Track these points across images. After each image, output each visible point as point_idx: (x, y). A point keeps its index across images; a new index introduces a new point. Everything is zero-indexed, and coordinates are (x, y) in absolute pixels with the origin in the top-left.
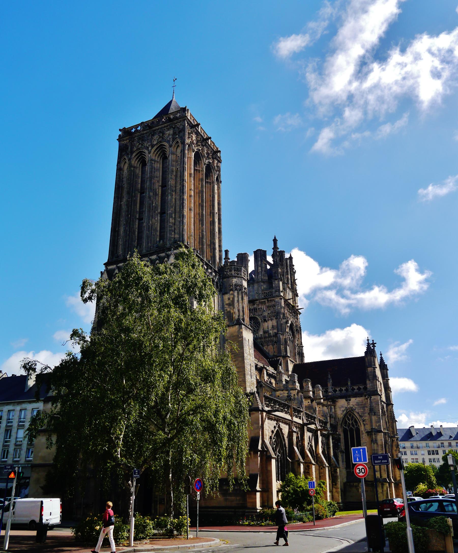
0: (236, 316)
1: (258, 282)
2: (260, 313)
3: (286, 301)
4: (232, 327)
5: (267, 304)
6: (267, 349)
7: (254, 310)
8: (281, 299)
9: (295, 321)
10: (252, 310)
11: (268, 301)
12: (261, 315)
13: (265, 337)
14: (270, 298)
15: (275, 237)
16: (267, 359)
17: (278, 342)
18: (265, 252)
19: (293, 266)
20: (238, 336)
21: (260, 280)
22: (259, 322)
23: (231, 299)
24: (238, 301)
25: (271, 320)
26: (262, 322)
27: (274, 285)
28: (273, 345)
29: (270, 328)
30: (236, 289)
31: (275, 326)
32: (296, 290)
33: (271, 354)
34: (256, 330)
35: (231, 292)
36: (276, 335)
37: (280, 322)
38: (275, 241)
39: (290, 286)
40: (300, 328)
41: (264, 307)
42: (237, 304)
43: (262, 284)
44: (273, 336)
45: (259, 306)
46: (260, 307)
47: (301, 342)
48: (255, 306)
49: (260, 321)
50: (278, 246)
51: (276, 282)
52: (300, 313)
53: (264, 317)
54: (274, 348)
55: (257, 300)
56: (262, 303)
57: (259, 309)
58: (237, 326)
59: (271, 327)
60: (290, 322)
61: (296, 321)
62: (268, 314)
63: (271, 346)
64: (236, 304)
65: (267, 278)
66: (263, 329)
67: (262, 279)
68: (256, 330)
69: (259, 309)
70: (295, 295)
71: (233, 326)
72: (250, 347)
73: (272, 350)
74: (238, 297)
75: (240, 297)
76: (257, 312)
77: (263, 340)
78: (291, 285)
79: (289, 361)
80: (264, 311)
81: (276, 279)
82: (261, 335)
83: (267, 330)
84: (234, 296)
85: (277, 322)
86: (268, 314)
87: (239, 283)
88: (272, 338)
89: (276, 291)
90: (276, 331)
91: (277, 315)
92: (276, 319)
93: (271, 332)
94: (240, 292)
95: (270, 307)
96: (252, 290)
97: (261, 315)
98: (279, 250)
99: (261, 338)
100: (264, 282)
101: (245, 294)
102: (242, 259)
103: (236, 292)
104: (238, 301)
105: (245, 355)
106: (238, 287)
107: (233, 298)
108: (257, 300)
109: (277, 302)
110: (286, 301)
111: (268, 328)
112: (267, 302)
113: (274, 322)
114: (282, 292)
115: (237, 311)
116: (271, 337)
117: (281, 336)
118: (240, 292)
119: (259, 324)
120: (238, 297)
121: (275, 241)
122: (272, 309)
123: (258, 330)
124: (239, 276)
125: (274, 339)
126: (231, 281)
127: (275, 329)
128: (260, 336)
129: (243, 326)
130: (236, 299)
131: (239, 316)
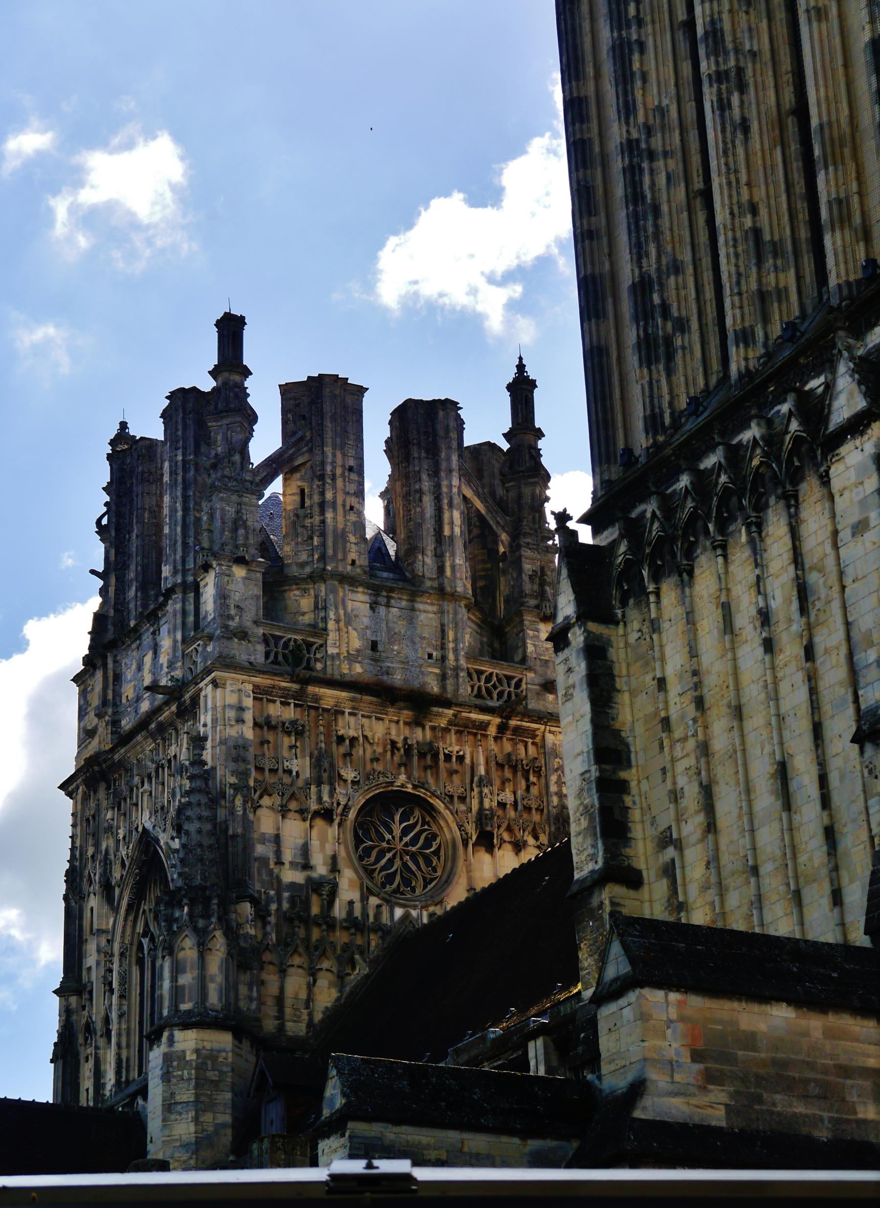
11: (502, 728)
15: (521, 367)
55: (448, 704)
112: (492, 731)
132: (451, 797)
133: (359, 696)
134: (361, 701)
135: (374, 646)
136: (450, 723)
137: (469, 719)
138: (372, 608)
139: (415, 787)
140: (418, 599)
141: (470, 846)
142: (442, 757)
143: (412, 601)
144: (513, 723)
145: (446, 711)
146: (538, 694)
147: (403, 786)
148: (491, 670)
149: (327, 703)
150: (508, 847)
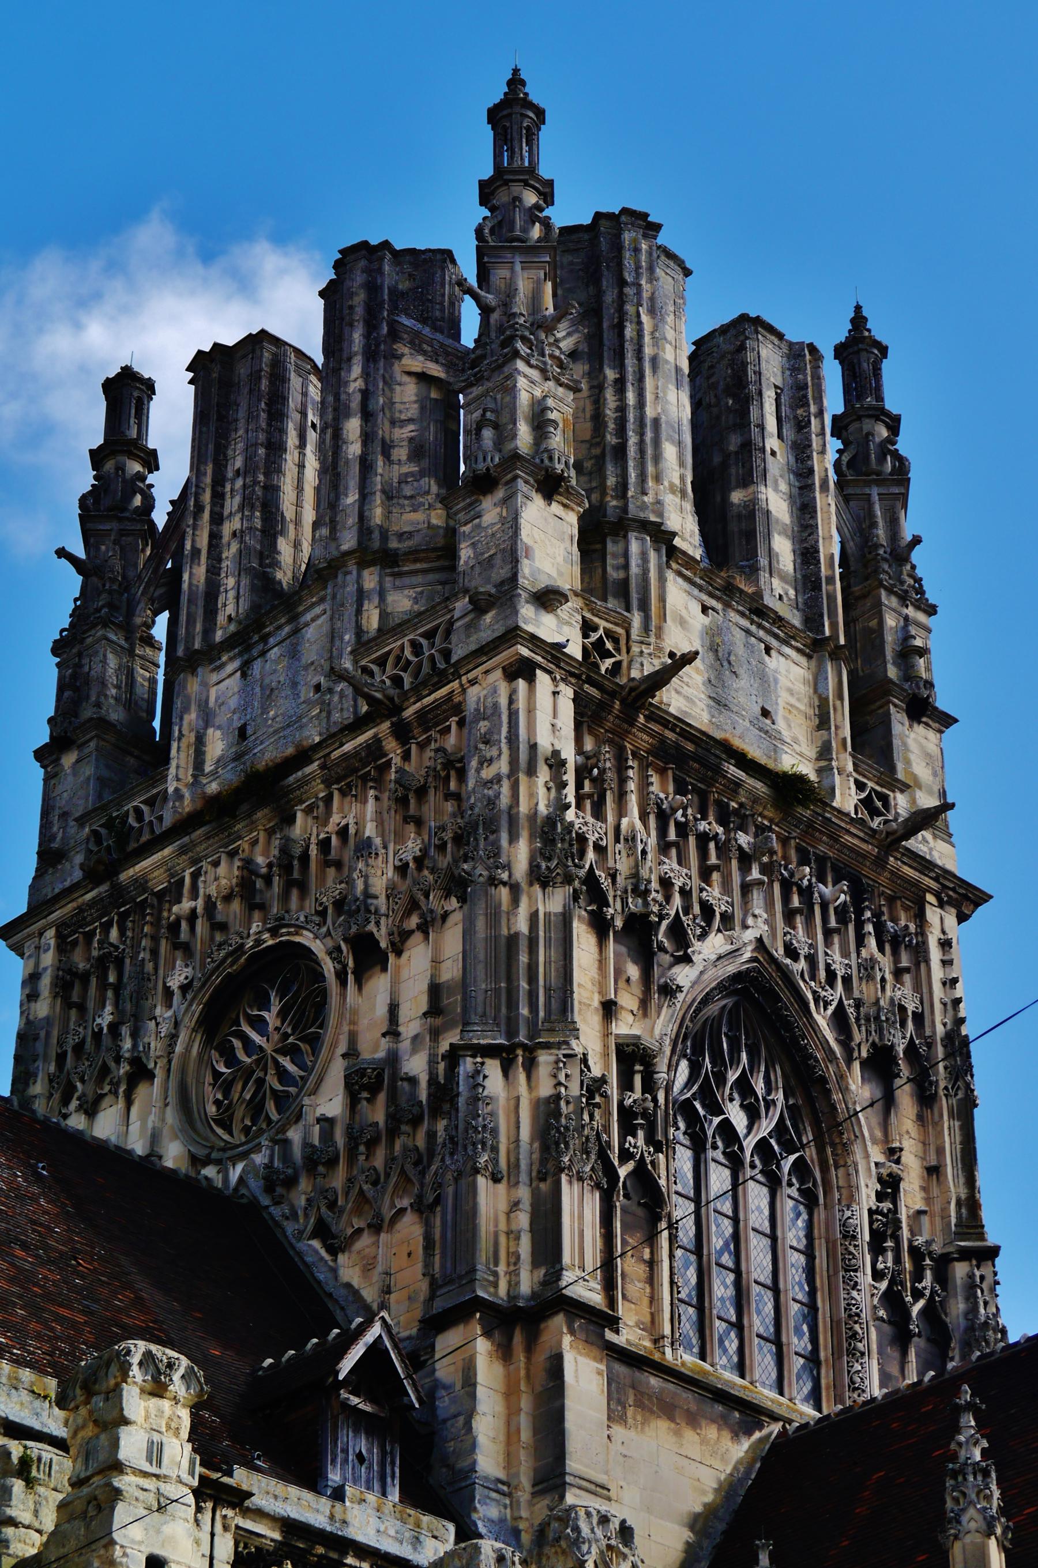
6: (368, 1268)
11: (402, 733)
14: (418, 691)
26: (341, 977)
29: (411, 1025)
37: (494, 916)
38: (514, 118)
40: (958, 1046)
47: (971, 1205)
50: (553, 154)
59: (423, 1004)
62: (402, 869)
66: (351, 1053)
69: (325, 845)
70: (882, 694)
76: (303, 887)
89: (480, 606)
93: (416, 1065)
99: (318, 1160)
108: (303, 756)
109: (480, 715)
110: (616, 704)
111: (393, 1032)
112: (392, 747)
114: (548, 599)
121: (514, 118)
133: (186, 839)
134: (193, 844)
137: (346, 757)
138: (244, 675)
139: (274, 932)
140: (301, 608)
141: (351, 978)
142: (313, 850)
143: (294, 618)
144: (409, 712)
145: (308, 770)
146: (468, 626)
147: (258, 942)
148: (399, 643)
149: (159, 882)
150: (418, 937)
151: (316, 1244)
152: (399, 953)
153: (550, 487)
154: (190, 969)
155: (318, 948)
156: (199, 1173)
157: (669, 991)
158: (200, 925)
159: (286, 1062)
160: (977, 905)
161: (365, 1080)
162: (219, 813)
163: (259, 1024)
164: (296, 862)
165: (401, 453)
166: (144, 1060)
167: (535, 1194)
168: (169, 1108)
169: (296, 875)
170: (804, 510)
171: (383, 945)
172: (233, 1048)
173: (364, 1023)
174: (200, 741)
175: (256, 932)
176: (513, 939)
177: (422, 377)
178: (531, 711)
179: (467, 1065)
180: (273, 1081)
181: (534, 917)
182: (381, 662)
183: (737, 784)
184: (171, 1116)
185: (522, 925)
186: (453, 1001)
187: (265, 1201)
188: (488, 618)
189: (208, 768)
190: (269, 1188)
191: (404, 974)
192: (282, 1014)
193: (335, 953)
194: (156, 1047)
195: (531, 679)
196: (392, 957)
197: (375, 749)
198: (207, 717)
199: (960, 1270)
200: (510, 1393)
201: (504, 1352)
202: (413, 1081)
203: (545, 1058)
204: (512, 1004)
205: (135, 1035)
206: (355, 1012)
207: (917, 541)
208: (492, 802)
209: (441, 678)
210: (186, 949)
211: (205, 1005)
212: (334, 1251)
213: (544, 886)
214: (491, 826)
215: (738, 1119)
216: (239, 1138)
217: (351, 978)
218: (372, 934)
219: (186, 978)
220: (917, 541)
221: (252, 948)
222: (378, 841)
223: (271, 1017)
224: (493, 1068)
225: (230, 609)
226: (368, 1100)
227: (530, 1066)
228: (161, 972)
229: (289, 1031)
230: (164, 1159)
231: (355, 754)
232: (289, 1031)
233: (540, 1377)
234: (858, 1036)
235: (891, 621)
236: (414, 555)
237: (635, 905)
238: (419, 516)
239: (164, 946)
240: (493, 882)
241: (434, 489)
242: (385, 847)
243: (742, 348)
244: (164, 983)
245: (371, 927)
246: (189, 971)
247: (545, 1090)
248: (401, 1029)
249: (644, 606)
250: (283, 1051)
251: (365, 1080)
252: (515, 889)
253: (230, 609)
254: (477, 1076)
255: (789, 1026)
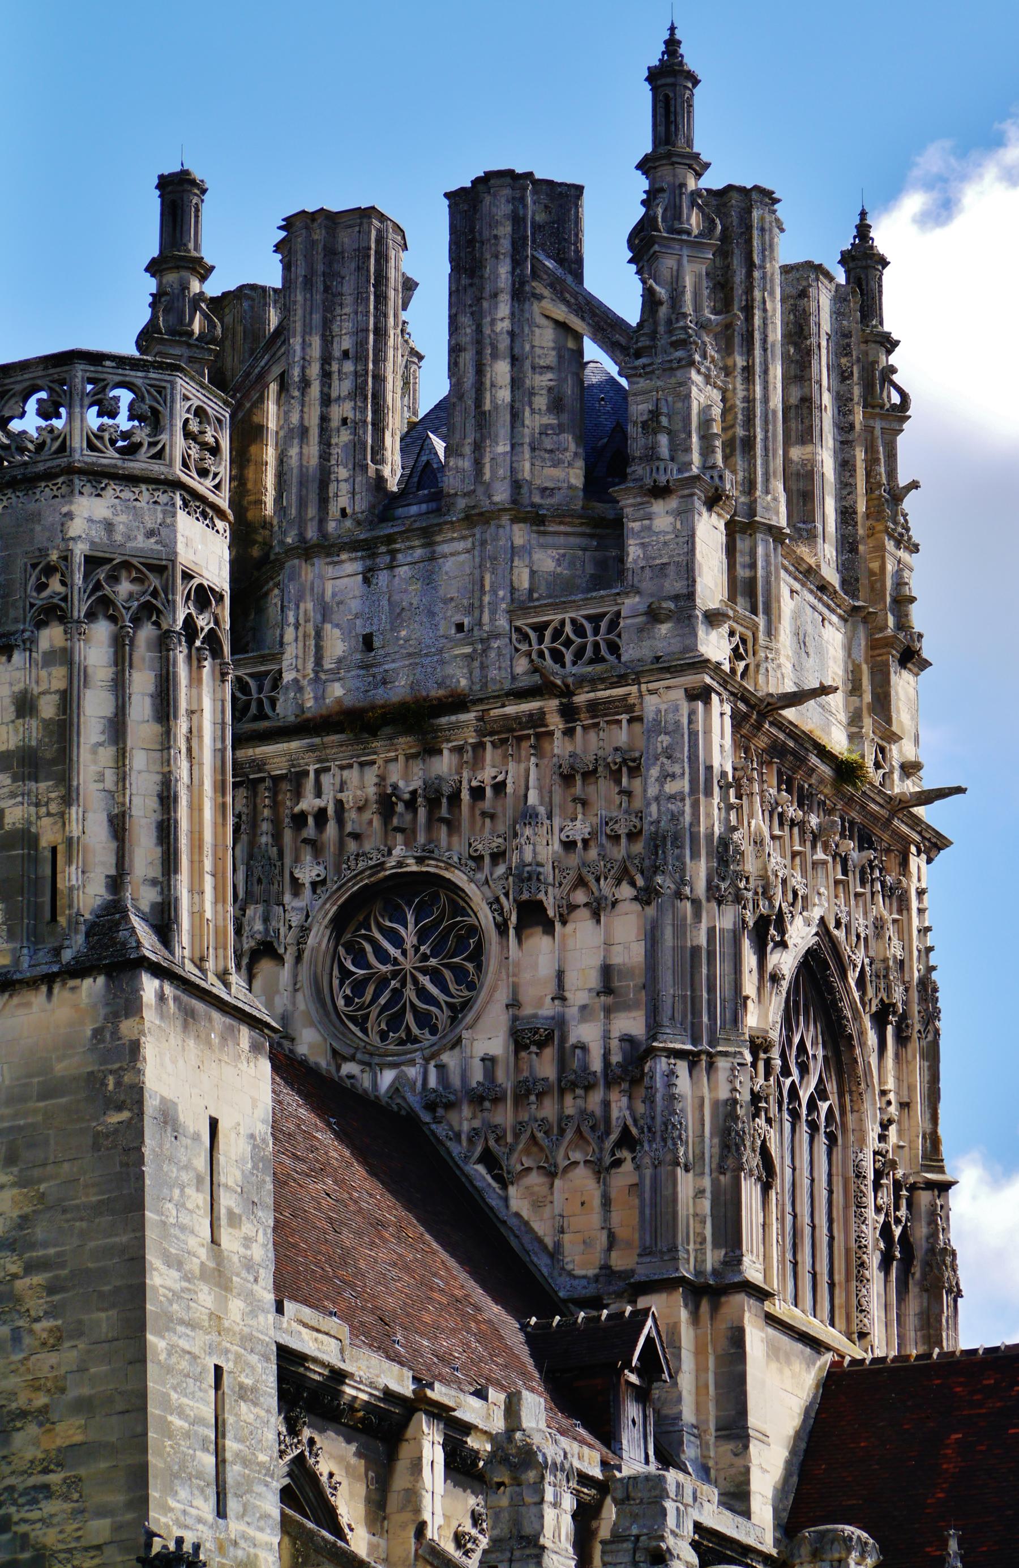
0: (86, 889)
1: (478, 518)
2: (486, 843)
3: (755, 714)
4: (38, 998)
5: (559, 747)
6: (537, 1205)
7: (433, 803)
8: (703, 695)
9: (861, 924)
10: (411, 805)
11: (569, 713)
12: (497, 857)
13: (527, 1091)
14: (593, 682)
15: (672, 44)
16: (519, 1314)
17: (642, 1141)
18: (564, 200)
19: (890, 344)
20: (93, 1081)
21: (501, 495)
22: (474, 930)
23: (48, 708)
24: (117, 727)
25: (597, 909)
26: (502, 929)
27: (634, 552)
28: (601, 1170)
30: (103, 606)
31: (626, 972)
32: (902, 602)
33: (581, 1260)
34: (442, 1016)
35: (51, 636)
36: (633, 1065)
37: (680, 929)
38: (670, 83)
39: (826, 557)
40: (927, 989)
41: (526, 776)
42: (107, 754)
43: (520, 534)
44: (611, 1078)
45: (477, 763)
46: (487, 774)
47: (933, 1141)
48: (444, 764)
49: (486, 918)
50: (708, 131)
51: (662, 516)
52: (935, 844)
53: (527, 876)
54: (606, 1202)
55: (458, 703)
56: (523, 735)
57: (477, 793)
58: (91, 988)
59: (594, 980)
60: (801, 934)
61: (879, 926)
62: (569, 845)
63: (582, 1179)
64: (92, 761)
65: (576, 477)
66: (514, 1004)
67: (516, 485)
68: (442, 1016)
69: (477, 793)
70: (888, 645)
71: (49, 980)
72: (227, 1201)
73: (595, 1218)
74: (119, 686)
75: (142, 682)
77: (505, 1116)
78: (848, 545)
79: (757, 1338)
80: (528, 816)
81: (660, 492)
82: (489, 1061)
83: (548, 1009)
84: (76, 676)
85: (652, 938)
86: (569, 845)
87: (141, 542)
88: (596, 1098)
89: (654, 615)
90: (632, 1023)
91: (647, 859)
92: (646, 896)
93: (587, 1033)
94: (146, 633)
95: (590, 775)
96: (412, 594)
97: (497, 857)
98: (712, 181)
99: (484, 1097)
100: (536, 519)
101: (195, 661)
102: (331, 275)
103: (102, 631)
104: (117, 727)
105: (160, 1278)
106: (125, 588)
107: (68, 701)
108: (458, 703)
109: (658, 728)
110: (755, 714)
111: (560, 997)
112: (555, 722)
113: (625, 934)
114: (713, 618)
115: (91, 828)
116: (573, 1079)
117: (683, 1083)
118: (146, 633)
119: (477, 956)
120: (119, 686)
121: (670, 83)
122: (603, 794)
123: (458, 1011)
124: (140, 464)
125: (619, 1107)
126: (51, 518)
127: (625, 1006)
128: (477, 1075)
129: (150, 986)
130: (95, 706)
131: (116, 883)
132: (479, 859)
133: (317, 740)
134: (325, 746)
135: (368, 642)
136: (481, 733)
137: (506, 717)
138: (367, 581)
139: (420, 860)
140: (439, 538)
141: (512, 932)
142: (465, 795)
143: (430, 544)
144: (581, 698)
145: (463, 717)
146: (641, 630)
147: (400, 864)
148: (560, 617)
149: (279, 768)
150: (584, 913)
151: (481, 1168)
152: (564, 923)
153: (713, 501)
154: (321, 868)
155: (471, 889)
156: (338, 1068)
157: (775, 978)
158: (331, 829)
159: (425, 981)
160: (939, 849)
161: (537, 1037)
162: (359, 725)
163: (398, 941)
164: (444, 800)
165: (541, 402)
166: (275, 944)
167: (715, 1183)
168: (300, 996)
169: (444, 812)
170: (845, 465)
171: (551, 913)
172: (363, 950)
173: (526, 976)
174: (319, 635)
175: (401, 857)
176: (696, 950)
177: (562, 326)
178: (708, 732)
179: (662, 1064)
180: (410, 993)
181: (711, 931)
182: (540, 629)
183: (813, 770)
184: (304, 1002)
185: (703, 941)
186: (630, 986)
187: (426, 1117)
188: (664, 628)
189: (328, 665)
190: (431, 1107)
191: (570, 943)
192: (422, 936)
193: (495, 903)
194: (287, 938)
195: (707, 702)
196: (558, 926)
197: (537, 719)
198: (325, 612)
199: (924, 1197)
200: (699, 1352)
201: (695, 1319)
202: (584, 1048)
203: (722, 1064)
204: (696, 1013)
205: (266, 920)
206: (517, 965)
207: (914, 485)
208: (675, 818)
209: (621, 680)
210: (315, 846)
211: (341, 907)
212: (504, 1183)
213: (720, 903)
214: (677, 840)
215: (796, 1075)
216: (375, 1039)
217: (512, 932)
218: (541, 902)
219: (318, 875)
220: (914, 485)
221: (393, 867)
222: (542, 810)
223: (409, 937)
224: (682, 1067)
225: (343, 501)
226: (537, 1054)
227: (711, 1066)
228: (288, 860)
229: (428, 952)
230: (298, 1041)
231: (517, 718)
232: (428, 952)
233: (723, 1343)
234: (870, 992)
235: (890, 567)
236: (561, 515)
237: (764, 909)
238: (557, 473)
239: (288, 835)
240: (679, 895)
241: (572, 447)
242: (550, 817)
243: (803, 294)
244: (291, 873)
245: (541, 896)
246: (319, 869)
247: (724, 1094)
248: (567, 994)
249: (767, 611)
250: (424, 971)
251: (537, 1037)
252: (696, 903)
253: (343, 501)
254: (672, 1073)
255: (831, 990)
